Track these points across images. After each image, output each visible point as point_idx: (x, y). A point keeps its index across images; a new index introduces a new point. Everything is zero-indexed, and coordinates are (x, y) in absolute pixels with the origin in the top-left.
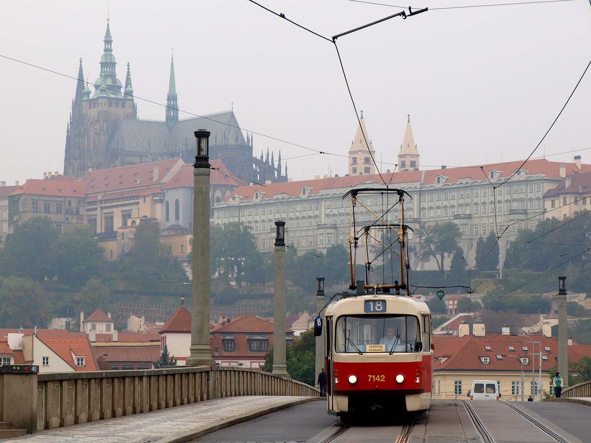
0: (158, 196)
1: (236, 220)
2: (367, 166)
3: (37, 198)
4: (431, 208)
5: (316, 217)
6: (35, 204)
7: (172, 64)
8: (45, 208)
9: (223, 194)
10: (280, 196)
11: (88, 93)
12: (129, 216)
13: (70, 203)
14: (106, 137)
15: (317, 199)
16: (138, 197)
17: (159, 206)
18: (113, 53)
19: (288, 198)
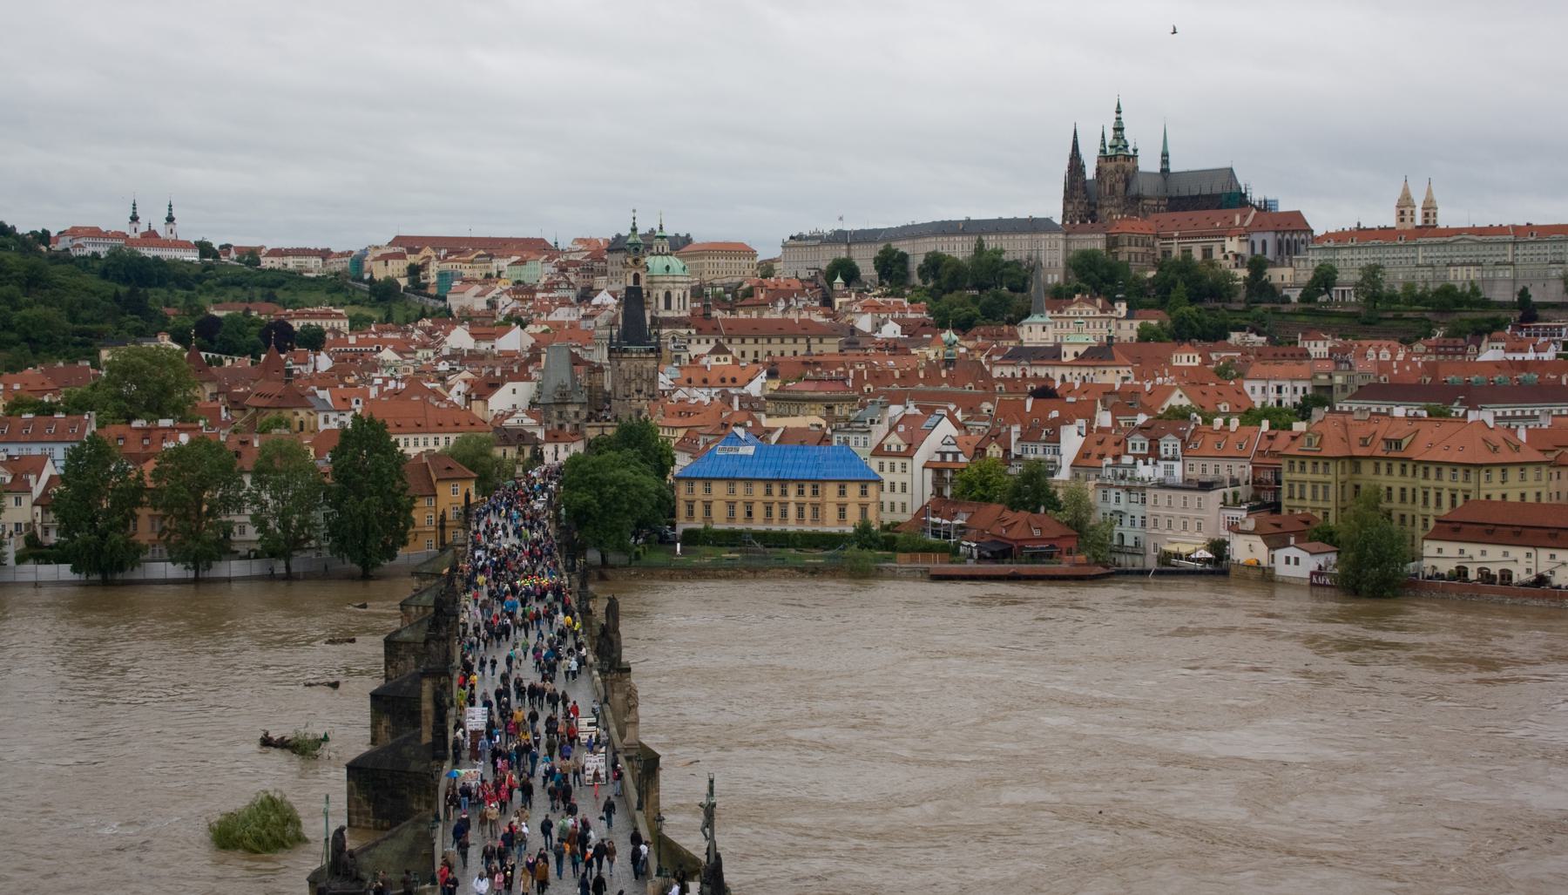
1: (1331, 257)
4: (1525, 255)
6: (1130, 240)
10: (1376, 242)
12: (1211, 250)
15: (1415, 246)
16: (1223, 236)
17: (1245, 243)
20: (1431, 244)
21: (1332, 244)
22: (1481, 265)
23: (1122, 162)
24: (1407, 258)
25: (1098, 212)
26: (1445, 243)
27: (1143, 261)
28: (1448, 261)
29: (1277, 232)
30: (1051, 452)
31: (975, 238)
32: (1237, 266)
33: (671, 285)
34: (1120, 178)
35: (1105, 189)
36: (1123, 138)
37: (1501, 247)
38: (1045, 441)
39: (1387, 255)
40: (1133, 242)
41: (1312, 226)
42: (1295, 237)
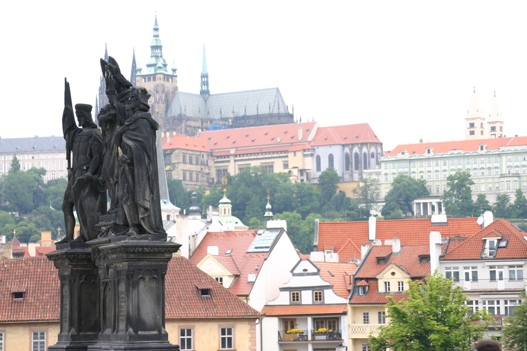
0: (309, 151)
1: (407, 170)
2: (482, 129)
3: (185, 152)
5: (496, 168)
7: (204, 49)
8: (190, 159)
9: (377, 150)
10: (456, 152)
11: (140, 70)
12: (272, 167)
13: (203, 155)
14: (165, 104)
15: (499, 154)
16: (285, 152)
18: (160, 38)
19: (464, 153)
21: (407, 156)
23: (162, 82)
24: (489, 168)
27: (197, 180)
29: (344, 146)
30: (506, 275)
31: (11, 158)
32: (302, 180)
34: (161, 97)
36: (161, 56)
38: (496, 259)
39: (467, 167)
40: (188, 160)
41: (381, 140)
42: (365, 150)
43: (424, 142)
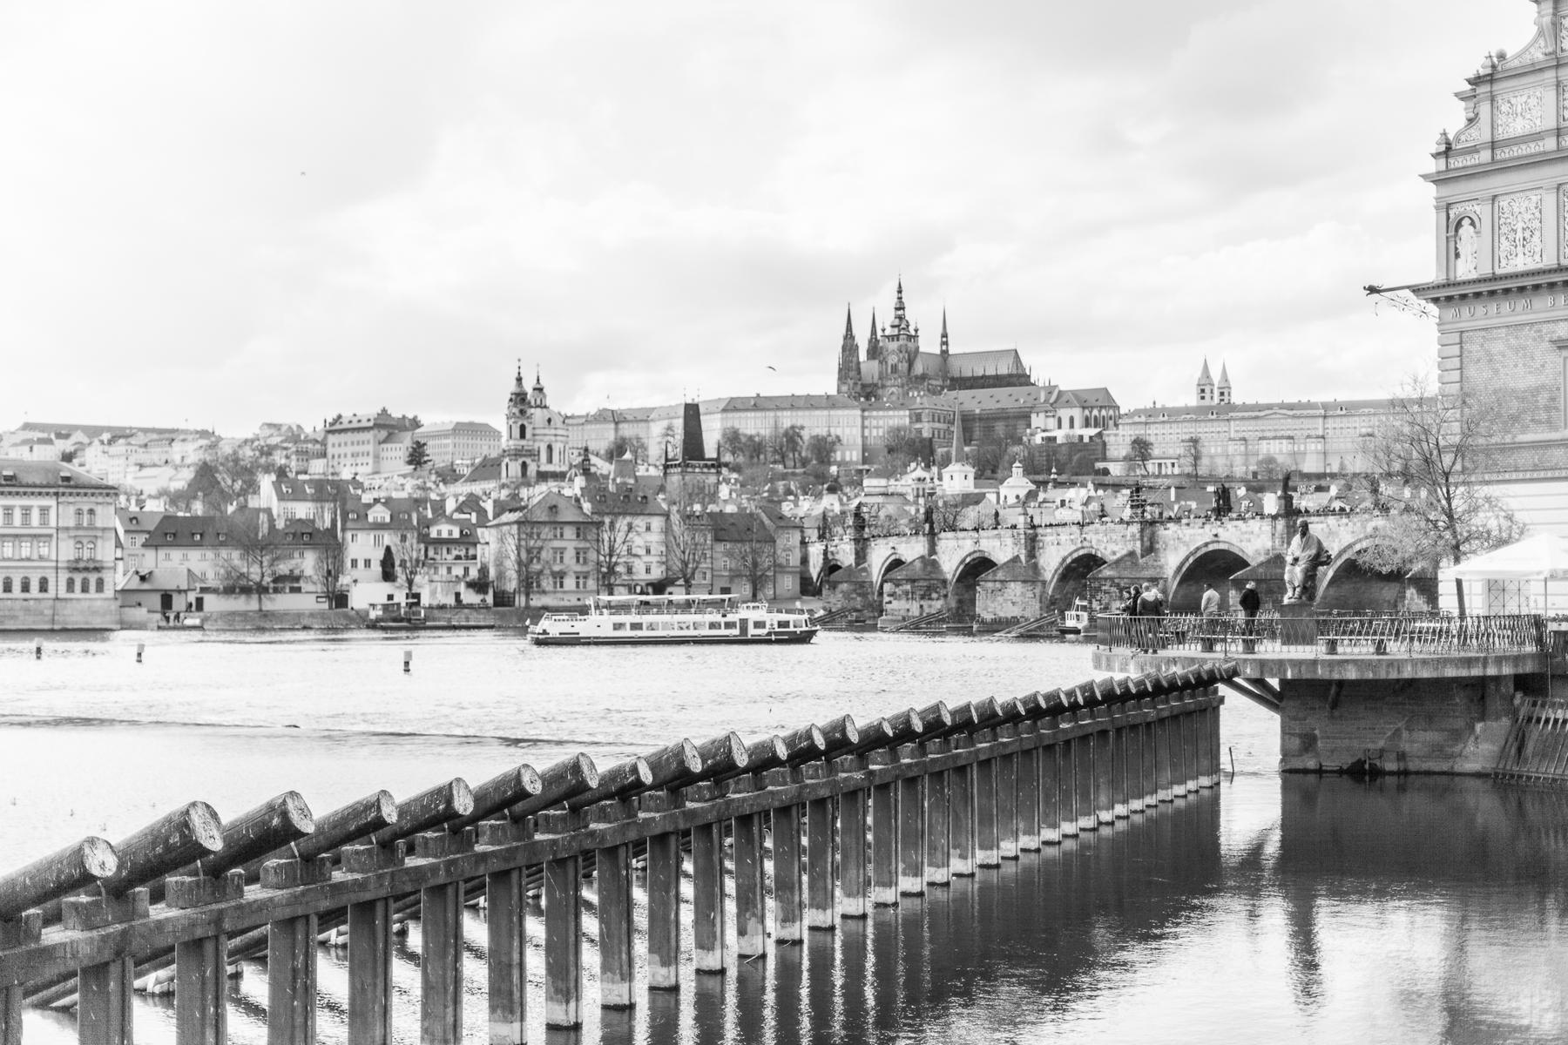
1: (1143, 432)
10: (1188, 416)
11: (883, 330)
17: (1052, 419)
20: (1243, 419)
21: (1143, 419)
22: (1291, 438)
24: (1219, 432)
25: (880, 392)
26: (1256, 418)
28: (1260, 434)
29: (1084, 408)
33: (553, 438)
35: (887, 369)
37: (1310, 421)
39: (1199, 430)
40: (936, 419)
42: (1104, 412)
43: (1158, 406)
